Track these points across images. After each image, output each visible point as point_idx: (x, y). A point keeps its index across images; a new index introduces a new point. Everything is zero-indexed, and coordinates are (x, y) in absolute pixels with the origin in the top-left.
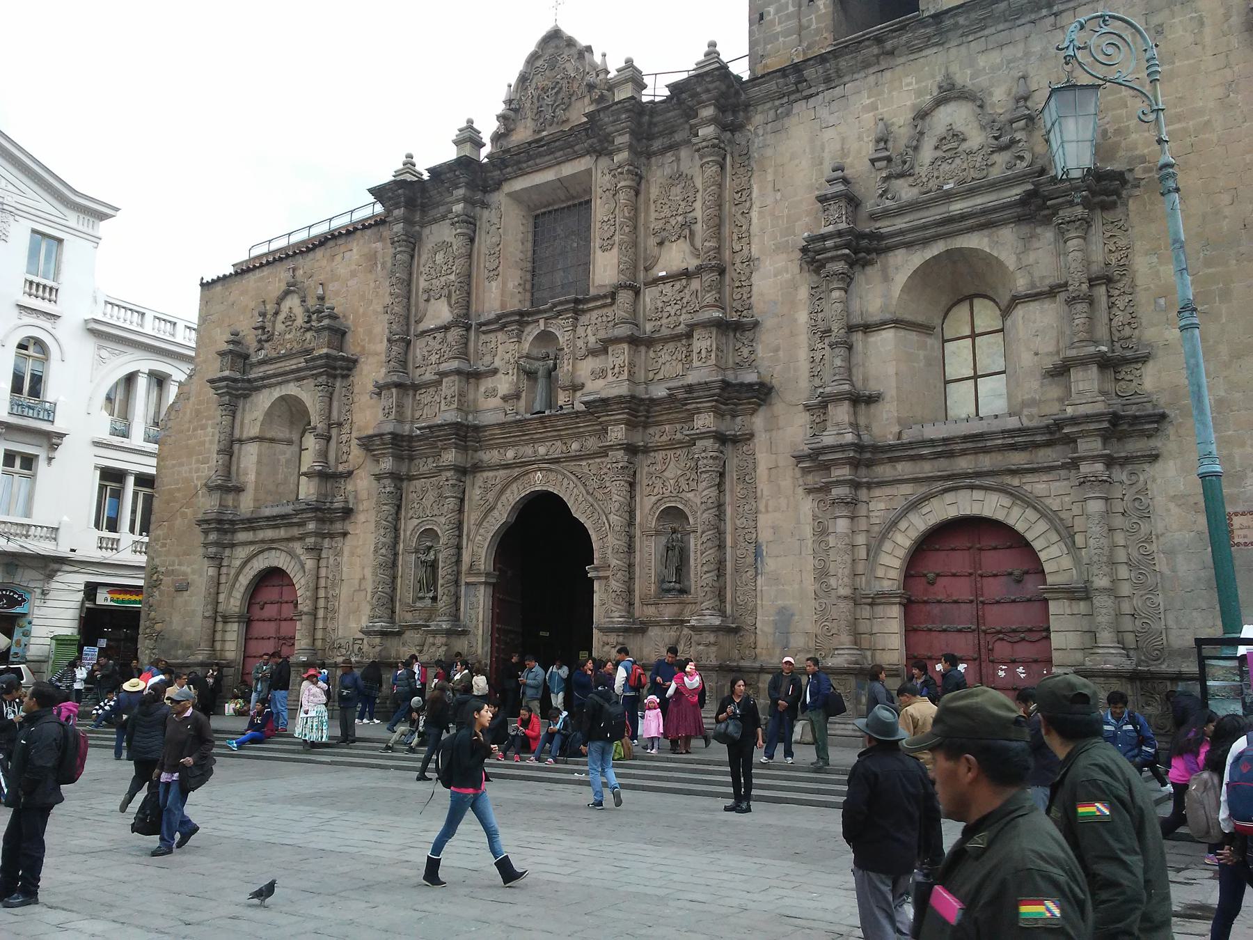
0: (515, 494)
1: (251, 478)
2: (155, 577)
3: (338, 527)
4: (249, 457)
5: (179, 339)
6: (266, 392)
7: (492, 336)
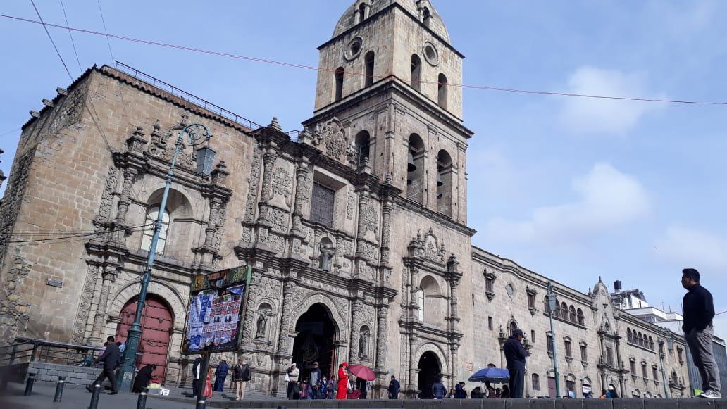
2: (20, 267)
6: (158, 179)
7: (308, 228)
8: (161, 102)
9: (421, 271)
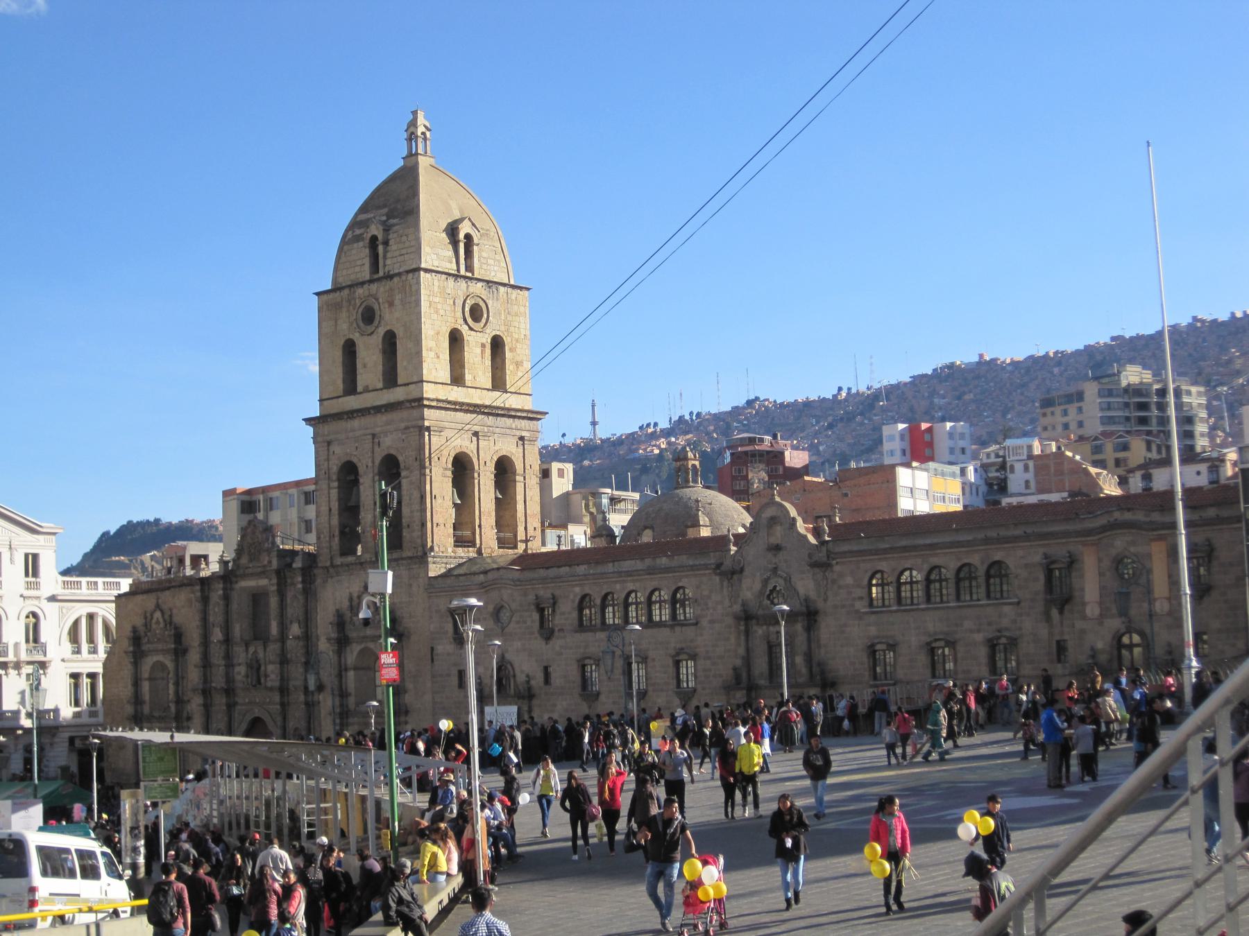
0: (249, 718)
1: (147, 698)
3: (185, 724)
4: (146, 686)
5: (101, 595)
6: (150, 657)
8: (145, 596)
9: (354, 645)
